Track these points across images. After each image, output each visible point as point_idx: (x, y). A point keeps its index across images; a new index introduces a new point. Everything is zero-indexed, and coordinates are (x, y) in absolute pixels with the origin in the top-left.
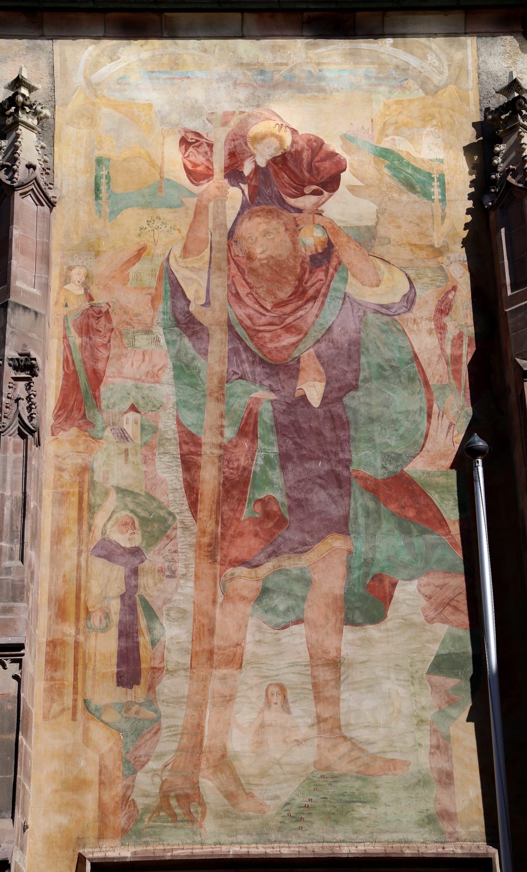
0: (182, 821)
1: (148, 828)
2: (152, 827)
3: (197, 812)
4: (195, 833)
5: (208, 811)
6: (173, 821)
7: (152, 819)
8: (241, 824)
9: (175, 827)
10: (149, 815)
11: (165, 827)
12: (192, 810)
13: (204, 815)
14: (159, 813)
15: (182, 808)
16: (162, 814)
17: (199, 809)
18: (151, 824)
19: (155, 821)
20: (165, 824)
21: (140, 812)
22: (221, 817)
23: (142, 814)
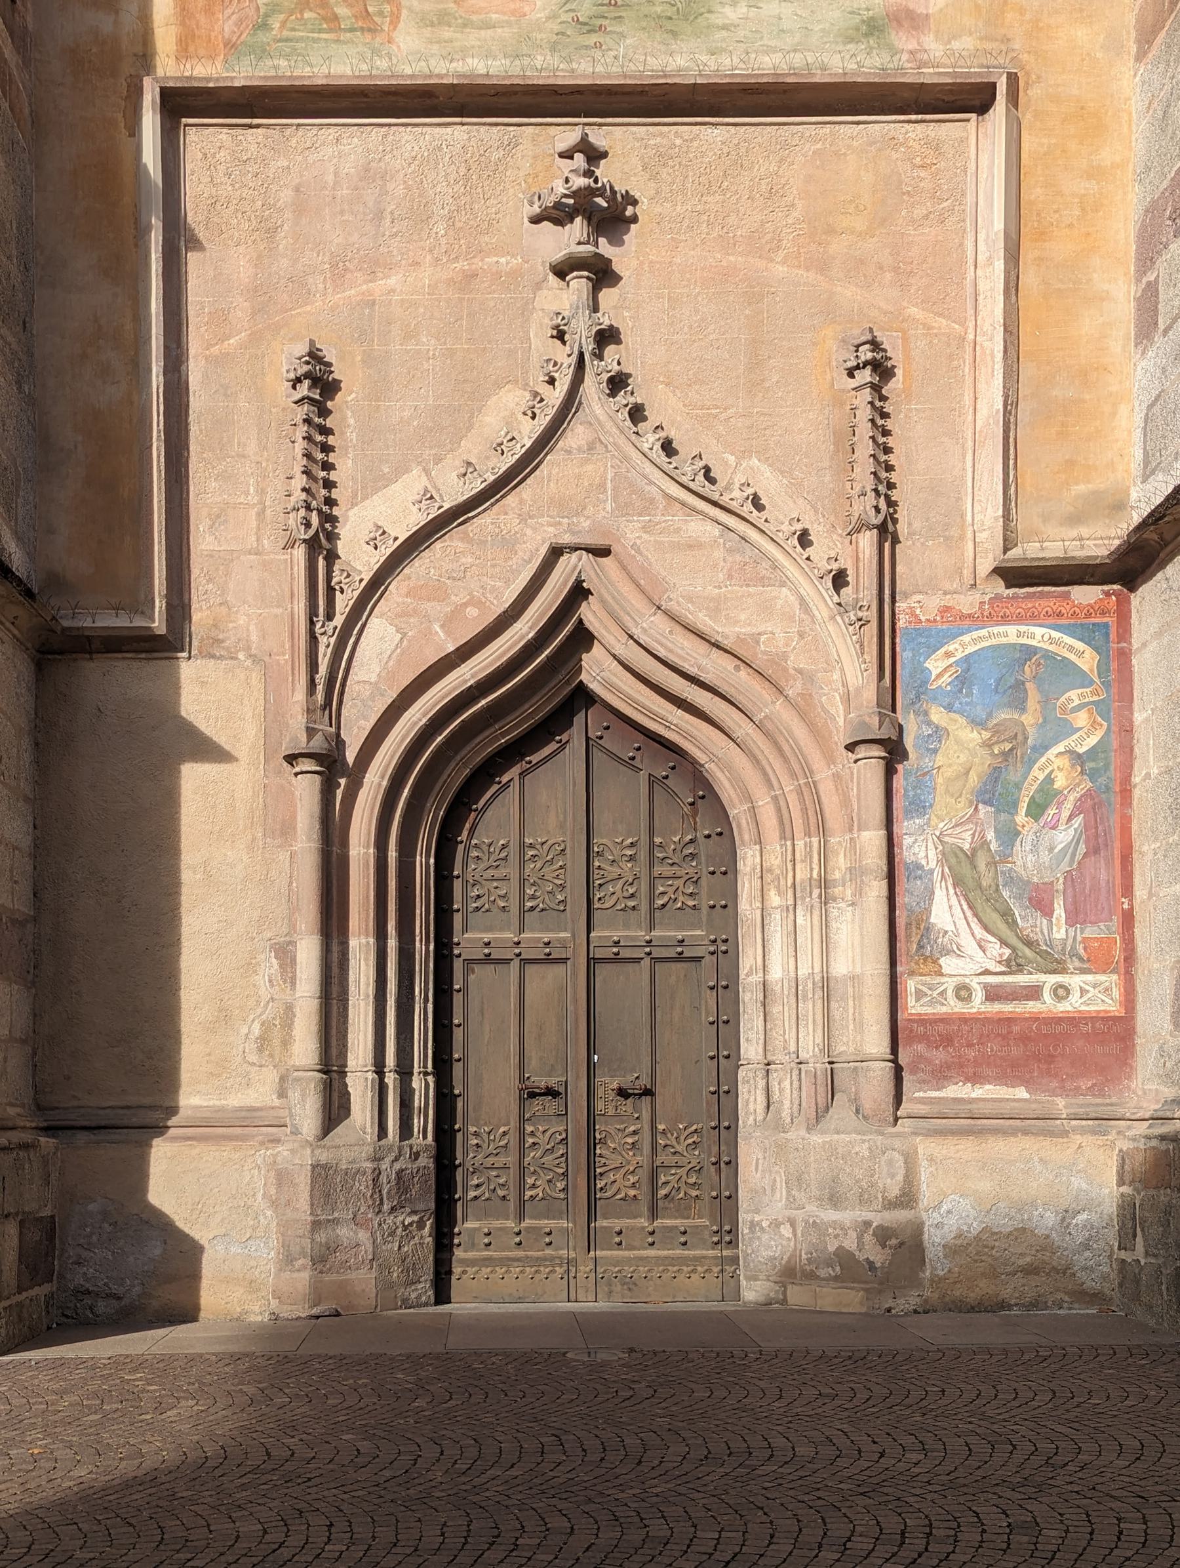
0: (352, 30)
1: (279, 41)
2: (287, 40)
3: (381, 13)
4: (376, 52)
5: (404, 12)
6: (330, 31)
7: (289, 25)
8: (472, 38)
9: (337, 41)
10: (282, 17)
11: (315, 40)
12: (370, 9)
13: (395, 20)
14: (302, 15)
15: (351, 6)
16: (307, 15)
17: (387, 8)
18: (286, 33)
19: (293, 29)
20: (316, 35)
21: (262, 11)
22: (432, 25)
23: (267, 15)
